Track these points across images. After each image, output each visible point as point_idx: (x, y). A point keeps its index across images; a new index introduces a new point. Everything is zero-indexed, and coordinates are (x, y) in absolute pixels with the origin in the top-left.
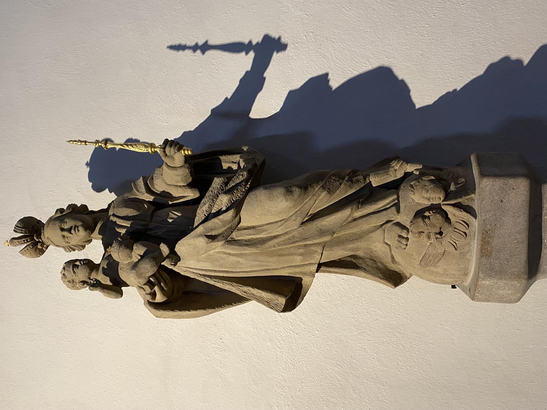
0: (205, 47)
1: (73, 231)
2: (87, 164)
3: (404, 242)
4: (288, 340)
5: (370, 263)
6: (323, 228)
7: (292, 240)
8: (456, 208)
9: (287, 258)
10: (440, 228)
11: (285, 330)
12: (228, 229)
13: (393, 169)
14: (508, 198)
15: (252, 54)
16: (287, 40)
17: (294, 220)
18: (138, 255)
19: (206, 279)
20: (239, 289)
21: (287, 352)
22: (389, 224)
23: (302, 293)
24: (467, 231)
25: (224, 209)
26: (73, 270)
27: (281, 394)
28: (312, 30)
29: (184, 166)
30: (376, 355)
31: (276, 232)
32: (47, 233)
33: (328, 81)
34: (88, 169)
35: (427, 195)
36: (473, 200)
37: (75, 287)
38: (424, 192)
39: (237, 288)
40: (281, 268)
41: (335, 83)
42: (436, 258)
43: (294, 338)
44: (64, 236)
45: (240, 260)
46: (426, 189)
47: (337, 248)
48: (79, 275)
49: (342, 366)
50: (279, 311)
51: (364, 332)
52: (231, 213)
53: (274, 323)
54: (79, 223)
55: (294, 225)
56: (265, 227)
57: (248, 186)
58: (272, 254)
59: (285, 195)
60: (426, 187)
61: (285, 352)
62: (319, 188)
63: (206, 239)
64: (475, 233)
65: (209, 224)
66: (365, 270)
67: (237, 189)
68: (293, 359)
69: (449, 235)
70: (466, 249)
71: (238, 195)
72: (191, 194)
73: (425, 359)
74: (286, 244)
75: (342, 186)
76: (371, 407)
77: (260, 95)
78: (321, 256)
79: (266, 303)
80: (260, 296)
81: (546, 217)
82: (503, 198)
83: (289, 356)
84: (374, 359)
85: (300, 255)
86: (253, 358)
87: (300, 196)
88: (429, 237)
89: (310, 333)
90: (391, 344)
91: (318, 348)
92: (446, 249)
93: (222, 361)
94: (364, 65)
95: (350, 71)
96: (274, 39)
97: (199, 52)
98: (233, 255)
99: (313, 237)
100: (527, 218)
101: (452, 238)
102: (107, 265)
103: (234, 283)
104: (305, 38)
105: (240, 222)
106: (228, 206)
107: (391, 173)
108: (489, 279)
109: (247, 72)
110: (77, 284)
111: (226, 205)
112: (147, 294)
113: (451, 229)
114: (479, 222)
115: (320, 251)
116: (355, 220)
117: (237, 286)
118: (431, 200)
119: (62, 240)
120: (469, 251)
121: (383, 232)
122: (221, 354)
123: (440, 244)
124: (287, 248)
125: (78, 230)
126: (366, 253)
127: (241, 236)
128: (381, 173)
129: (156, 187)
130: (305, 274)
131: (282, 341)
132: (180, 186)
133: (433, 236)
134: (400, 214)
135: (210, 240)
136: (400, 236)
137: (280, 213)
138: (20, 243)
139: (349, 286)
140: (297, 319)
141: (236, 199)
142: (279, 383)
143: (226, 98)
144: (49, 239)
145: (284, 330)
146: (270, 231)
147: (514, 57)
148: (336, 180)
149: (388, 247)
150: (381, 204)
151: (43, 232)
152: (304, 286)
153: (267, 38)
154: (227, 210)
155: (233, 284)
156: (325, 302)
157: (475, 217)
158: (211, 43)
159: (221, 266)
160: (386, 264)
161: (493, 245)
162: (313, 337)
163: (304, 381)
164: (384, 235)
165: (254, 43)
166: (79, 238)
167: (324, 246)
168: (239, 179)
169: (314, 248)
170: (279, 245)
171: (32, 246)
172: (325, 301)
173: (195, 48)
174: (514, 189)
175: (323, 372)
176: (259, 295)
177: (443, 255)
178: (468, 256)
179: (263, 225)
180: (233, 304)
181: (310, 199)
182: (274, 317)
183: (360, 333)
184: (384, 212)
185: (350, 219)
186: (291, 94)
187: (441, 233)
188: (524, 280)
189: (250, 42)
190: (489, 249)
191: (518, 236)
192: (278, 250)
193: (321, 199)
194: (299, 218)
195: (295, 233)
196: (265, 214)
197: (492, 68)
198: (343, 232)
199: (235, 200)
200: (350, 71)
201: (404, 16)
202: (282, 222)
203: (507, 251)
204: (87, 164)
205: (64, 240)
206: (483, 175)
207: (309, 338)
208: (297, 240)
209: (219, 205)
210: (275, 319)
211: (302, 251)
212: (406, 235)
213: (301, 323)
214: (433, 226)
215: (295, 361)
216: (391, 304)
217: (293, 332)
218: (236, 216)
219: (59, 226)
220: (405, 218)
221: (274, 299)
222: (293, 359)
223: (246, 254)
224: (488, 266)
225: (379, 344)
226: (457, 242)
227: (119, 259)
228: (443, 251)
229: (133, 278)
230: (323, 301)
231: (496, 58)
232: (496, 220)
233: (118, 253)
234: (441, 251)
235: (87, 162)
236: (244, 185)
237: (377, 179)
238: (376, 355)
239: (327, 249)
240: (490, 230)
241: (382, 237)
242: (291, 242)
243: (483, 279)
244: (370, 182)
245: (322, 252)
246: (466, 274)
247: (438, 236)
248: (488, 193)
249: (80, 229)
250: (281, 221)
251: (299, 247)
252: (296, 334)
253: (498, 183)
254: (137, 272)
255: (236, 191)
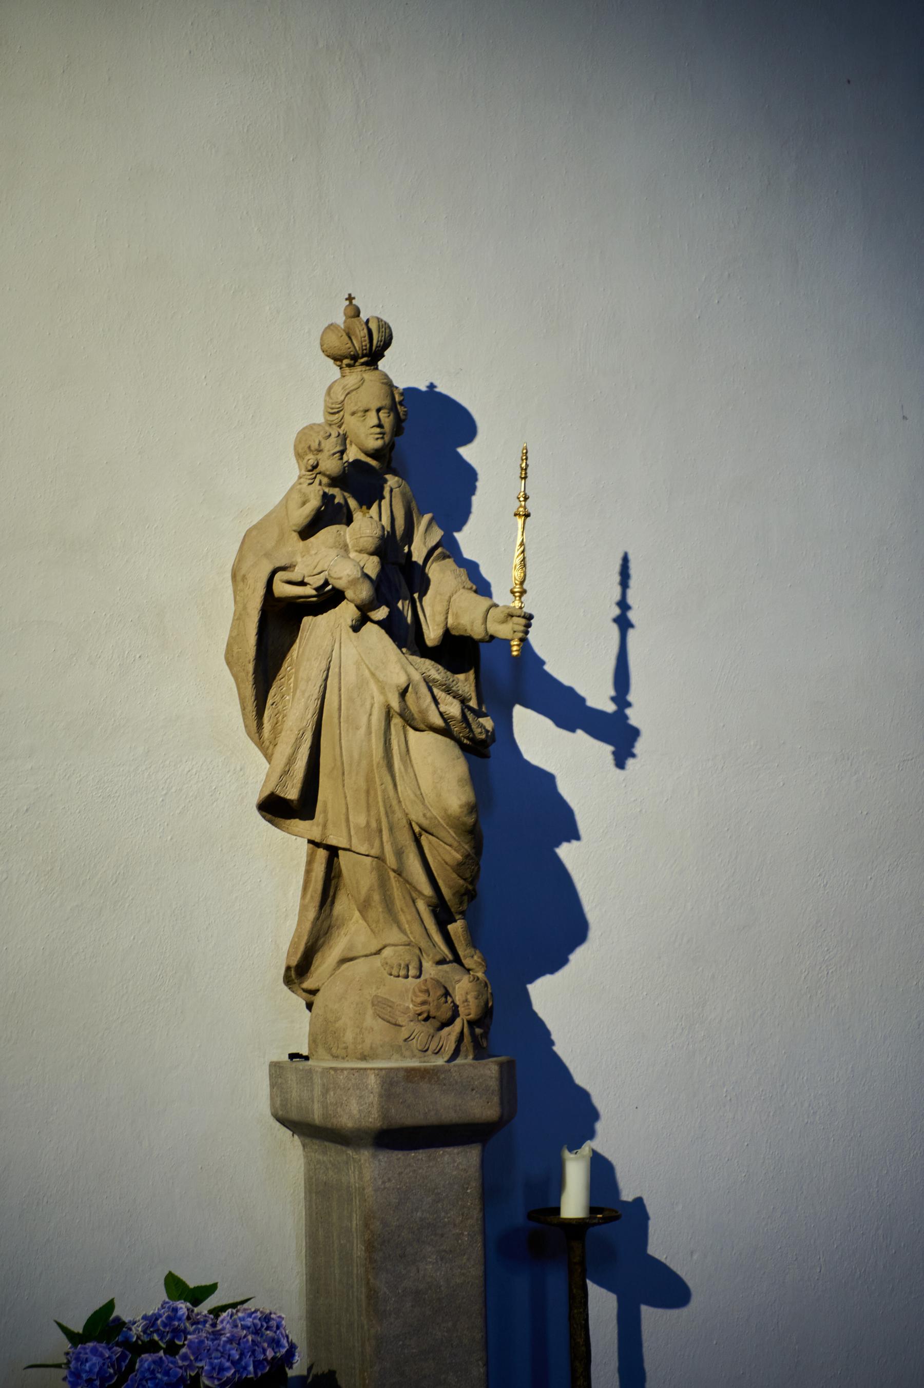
0: (623, 623)
1: (378, 430)
2: (432, 386)
3: (402, 973)
4: (151, 785)
5: (326, 925)
6: (404, 855)
7: (389, 812)
8: (458, 1035)
9: (363, 801)
10: (434, 1018)
11: (167, 779)
12: (413, 715)
13: (473, 952)
14: (477, 1097)
15: (610, 708)
16: (631, 768)
17: (424, 815)
18: (364, 565)
19: (324, 672)
20: (308, 724)
21: (131, 783)
22: (418, 951)
23: (278, 820)
24: (429, 1052)
25: (442, 709)
26: (338, 452)
27: (54, 774)
28: (644, 811)
29: (487, 634)
30: (140, 942)
31: (405, 787)
32: (371, 381)
33: (568, 841)
34: (423, 388)
35: (471, 998)
36: (466, 1057)
37: (308, 451)
38: (476, 993)
39: (309, 721)
40: (345, 793)
41: (566, 852)
42: (390, 1016)
43: (155, 796)
44: (367, 411)
45: (363, 730)
46: (479, 996)
47: (375, 877)
48: (329, 461)
49: (116, 884)
50: (276, 790)
51: (176, 920)
52: (438, 722)
53: (177, 757)
54: (387, 438)
55: (417, 815)
56: (410, 770)
57: (465, 741)
58: (369, 780)
59: (468, 804)
60: (481, 996)
61: (130, 780)
62: (466, 850)
63: (405, 685)
64: (428, 1062)
65: (424, 690)
66: (317, 918)
67: (465, 728)
68: (119, 796)
69: (421, 1030)
70: (407, 1053)
71: (456, 728)
72: (432, 634)
73: (141, 1026)
74: (384, 802)
75: (461, 882)
76: (52, 938)
77: (547, 723)
78: (364, 853)
79: (287, 769)
80: (298, 758)
81: (441, 1152)
82: (476, 1092)
83: (123, 787)
84: (134, 938)
85: (368, 823)
86: (113, 720)
87: (464, 824)
88: (424, 1003)
89: (167, 825)
90: (162, 967)
91: (142, 840)
92: (403, 1029)
93: (100, 660)
94: (592, 898)
95: (583, 876)
96: (632, 746)
97: (617, 611)
98: (369, 721)
99: (394, 843)
100: (454, 1121)
101: (420, 1034)
102: (339, 503)
103: (316, 717)
104: (633, 799)
105: (416, 729)
106: (444, 714)
107: (468, 951)
108: (378, 1082)
109: (582, 700)
110: (313, 455)
111: (447, 713)
112: (304, 577)
113: (432, 1031)
114: (443, 1065)
115: (373, 852)
116: (414, 902)
117: (313, 721)
118: (466, 1004)
119: (362, 406)
120: (404, 1057)
121: (407, 943)
122: (114, 656)
123: (411, 1019)
124: (378, 802)
125: (377, 439)
126: (337, 919)
127: (396, 731)
128: (467, 935)
129: (435, 565)
130: (325, 826)
131: (149, 774)
132: (447, 618)
133: (425, 1008)
134: (434, 965)
135: (401, 691)
136: (407, 967)
137: (439, 795)
138: (363, 339)
139: (250, 891)
140: (188, 801)
141: (452, 725)
142: (74, 770)
143: (543, 663)
144: (362, 384)
145: (166, 777)
146: (405, 778)
147: (599, 1126)
148: (472, 872)
149: (373, 951)
150: (437, 938)
151: (370, 369)
152: (288, 821)
153: (635, 733)
154: (441, 714)
155: (315, 715)
156: (220, 849)
157: (449, 1061)
158: (631, 634)
159: (351, 700)
160: (321, 950)
161: (421, 1084)
162: (161, 831)
163: (83, 817)
164: (401, 945)
165: (628, 712)
166: (363, 436)
167: (380, 858)
168: (477, 727)
169: (377, 843)
170: (384, 791)
171: (354, 355)
172: (222, 850)
173: (623, 605)
174: (488, 1102)
175: (103, 850)
176: (299, 756)
177: (396, 1025)
178: (396, 1056)
179: (412, 766)
180: (256, 702)
181: (455, 839)
182: (187, 757)
183: (174, 912)
184: (431, 944)
185: (414, 895)
186: (548, 779)
187: (426, 1019)
188: (381, 1125)
189: (629, 705)
190: (416, 1079)
191: (433, 1113)
192: (376, 790)
193: (450, 853)
194: (428, 822)
195: (399, 815)
196: (434, 772)
197: (583, 1096)
198: (398, 885)
199: (451, 723)
200: (583, 876)
201: (660, 958)
202: (421, 796)
203: (415, 1101)
204: (432, 386)
205: (362, 411)
206: (501, 1065)
207: (158, 824)
208: (390, 817)
209: (445, 699)
210: (185, 761)
211: (374, 824)
212: (413, 975)
213: (181, 807)
214: (438, 1007)
215: (115, 799)
216: (227, 963)
217: (166, 794)
218: (426, 726)
219: (386, 405)
220: (433, 972)
221: (295, 781)
222: (119, 796)
223: (369, 740)
224: (395, 1079)
225: (159, 946)
226: (414, 1040)
227: (359, 536)
228: (401, 1024)
229: (350, 573)
230: (221, 846)
231: (598, 1101)
232: (450, 1085)
233: (371, 535)
234: (400, 1021)
235: (435, 387)
236: (468, 736)
237: (460, 930)
238: (141, 943)
239: (374, 863)
240: (438, 1078)
241: (396, 942)
242: (388, 810)
243: (378, 1075)
244: (455, 921)
245: (371, 855)
246: (364, 1058)
247: (425, 1015)
248: (482, 1072)
249: (379, 443)
250: (421, 794)
251: (379, 821)
252: (163, 800)
253: (494, 1084)
254: (358, 579)
255: (464, 725)
